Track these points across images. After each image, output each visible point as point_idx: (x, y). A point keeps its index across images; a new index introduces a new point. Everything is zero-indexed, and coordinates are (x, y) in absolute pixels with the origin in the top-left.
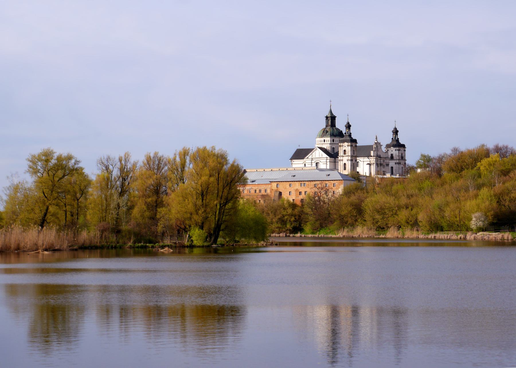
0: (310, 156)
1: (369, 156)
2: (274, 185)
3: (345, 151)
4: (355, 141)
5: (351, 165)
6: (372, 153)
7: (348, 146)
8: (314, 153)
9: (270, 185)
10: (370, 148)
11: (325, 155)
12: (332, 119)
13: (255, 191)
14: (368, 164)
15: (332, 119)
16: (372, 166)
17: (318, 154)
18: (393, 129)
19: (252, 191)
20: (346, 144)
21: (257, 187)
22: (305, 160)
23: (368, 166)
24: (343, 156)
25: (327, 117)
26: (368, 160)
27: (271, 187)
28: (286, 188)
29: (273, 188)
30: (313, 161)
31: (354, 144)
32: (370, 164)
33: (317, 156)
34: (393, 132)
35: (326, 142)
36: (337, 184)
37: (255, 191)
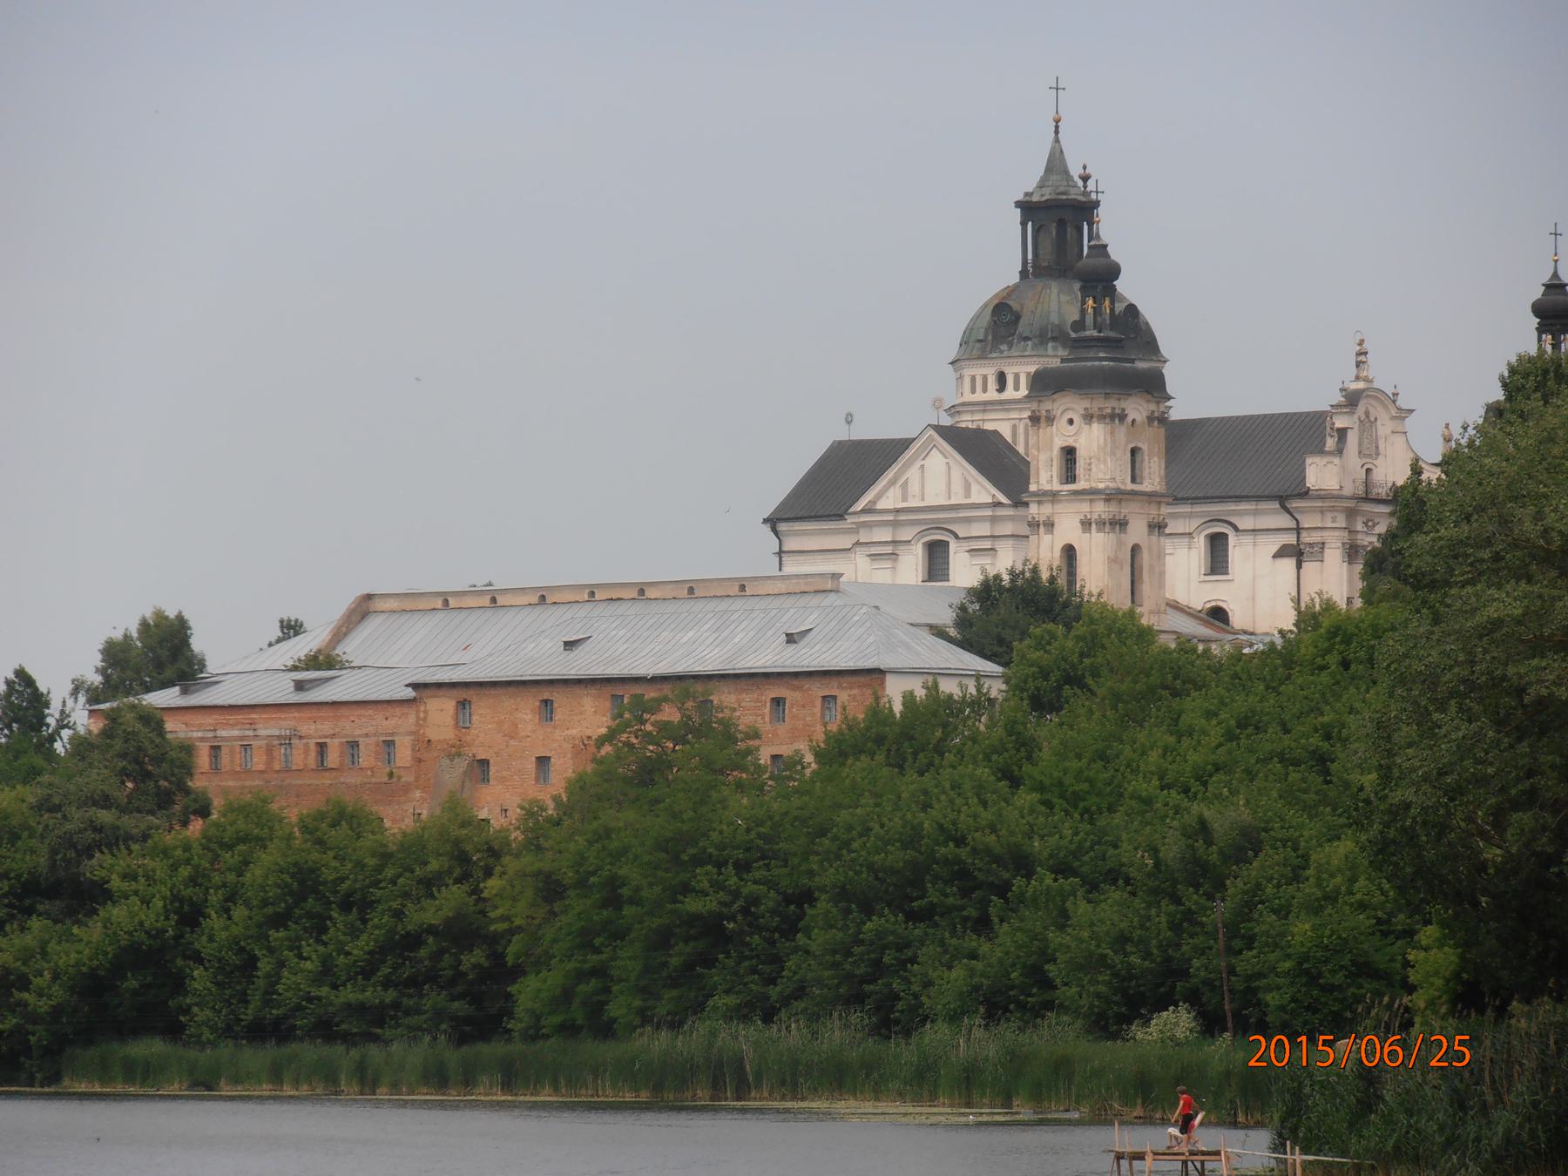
0: (886, 495)
1: (1290, 494)
2: (441, 711)
3: (1069, 453)
4: (1153, 386)
5: (1113, 561)
6: (1321, 474)
7: (1088, 418)
8: (913, 474)
9: (410, 719)
10: (1306, 432)
11: (983, 491)
12: (1060, 223)
13: (322, 747)
14: (1281, 553)
15: (1061, 223)
16: (1308, 567)
17: (938, 479)
18: (1537, 293)
19: (302, 756)
20: (1068, 406)
21: (326, 727)
22: (850, 519)
23: (1289, 564)
24: (1053, 496)
25: (1029, 209)
26: (1284, 521)
27: (422, 722)
28: (512, 735)
29: (433, 734)
30: (906, 534)
31: (1137, 409)
32: (1296, 553)
33: (936, 496)
34: (1538, 309)
35: (1010, 393)
36: (843, 697)
37: (322, 747)
